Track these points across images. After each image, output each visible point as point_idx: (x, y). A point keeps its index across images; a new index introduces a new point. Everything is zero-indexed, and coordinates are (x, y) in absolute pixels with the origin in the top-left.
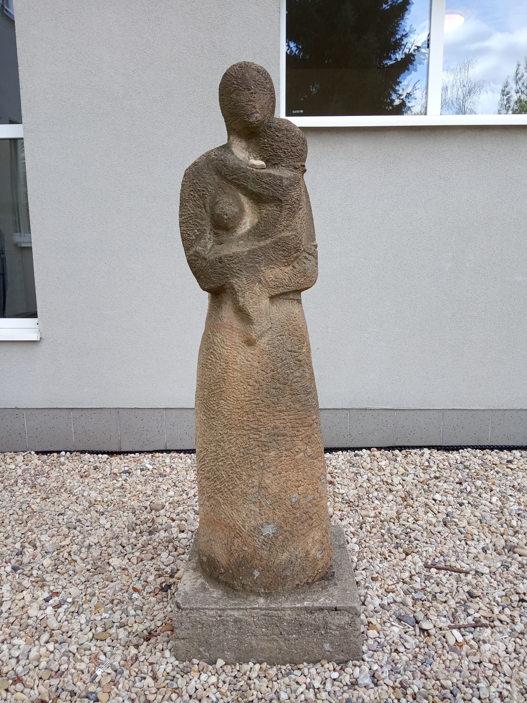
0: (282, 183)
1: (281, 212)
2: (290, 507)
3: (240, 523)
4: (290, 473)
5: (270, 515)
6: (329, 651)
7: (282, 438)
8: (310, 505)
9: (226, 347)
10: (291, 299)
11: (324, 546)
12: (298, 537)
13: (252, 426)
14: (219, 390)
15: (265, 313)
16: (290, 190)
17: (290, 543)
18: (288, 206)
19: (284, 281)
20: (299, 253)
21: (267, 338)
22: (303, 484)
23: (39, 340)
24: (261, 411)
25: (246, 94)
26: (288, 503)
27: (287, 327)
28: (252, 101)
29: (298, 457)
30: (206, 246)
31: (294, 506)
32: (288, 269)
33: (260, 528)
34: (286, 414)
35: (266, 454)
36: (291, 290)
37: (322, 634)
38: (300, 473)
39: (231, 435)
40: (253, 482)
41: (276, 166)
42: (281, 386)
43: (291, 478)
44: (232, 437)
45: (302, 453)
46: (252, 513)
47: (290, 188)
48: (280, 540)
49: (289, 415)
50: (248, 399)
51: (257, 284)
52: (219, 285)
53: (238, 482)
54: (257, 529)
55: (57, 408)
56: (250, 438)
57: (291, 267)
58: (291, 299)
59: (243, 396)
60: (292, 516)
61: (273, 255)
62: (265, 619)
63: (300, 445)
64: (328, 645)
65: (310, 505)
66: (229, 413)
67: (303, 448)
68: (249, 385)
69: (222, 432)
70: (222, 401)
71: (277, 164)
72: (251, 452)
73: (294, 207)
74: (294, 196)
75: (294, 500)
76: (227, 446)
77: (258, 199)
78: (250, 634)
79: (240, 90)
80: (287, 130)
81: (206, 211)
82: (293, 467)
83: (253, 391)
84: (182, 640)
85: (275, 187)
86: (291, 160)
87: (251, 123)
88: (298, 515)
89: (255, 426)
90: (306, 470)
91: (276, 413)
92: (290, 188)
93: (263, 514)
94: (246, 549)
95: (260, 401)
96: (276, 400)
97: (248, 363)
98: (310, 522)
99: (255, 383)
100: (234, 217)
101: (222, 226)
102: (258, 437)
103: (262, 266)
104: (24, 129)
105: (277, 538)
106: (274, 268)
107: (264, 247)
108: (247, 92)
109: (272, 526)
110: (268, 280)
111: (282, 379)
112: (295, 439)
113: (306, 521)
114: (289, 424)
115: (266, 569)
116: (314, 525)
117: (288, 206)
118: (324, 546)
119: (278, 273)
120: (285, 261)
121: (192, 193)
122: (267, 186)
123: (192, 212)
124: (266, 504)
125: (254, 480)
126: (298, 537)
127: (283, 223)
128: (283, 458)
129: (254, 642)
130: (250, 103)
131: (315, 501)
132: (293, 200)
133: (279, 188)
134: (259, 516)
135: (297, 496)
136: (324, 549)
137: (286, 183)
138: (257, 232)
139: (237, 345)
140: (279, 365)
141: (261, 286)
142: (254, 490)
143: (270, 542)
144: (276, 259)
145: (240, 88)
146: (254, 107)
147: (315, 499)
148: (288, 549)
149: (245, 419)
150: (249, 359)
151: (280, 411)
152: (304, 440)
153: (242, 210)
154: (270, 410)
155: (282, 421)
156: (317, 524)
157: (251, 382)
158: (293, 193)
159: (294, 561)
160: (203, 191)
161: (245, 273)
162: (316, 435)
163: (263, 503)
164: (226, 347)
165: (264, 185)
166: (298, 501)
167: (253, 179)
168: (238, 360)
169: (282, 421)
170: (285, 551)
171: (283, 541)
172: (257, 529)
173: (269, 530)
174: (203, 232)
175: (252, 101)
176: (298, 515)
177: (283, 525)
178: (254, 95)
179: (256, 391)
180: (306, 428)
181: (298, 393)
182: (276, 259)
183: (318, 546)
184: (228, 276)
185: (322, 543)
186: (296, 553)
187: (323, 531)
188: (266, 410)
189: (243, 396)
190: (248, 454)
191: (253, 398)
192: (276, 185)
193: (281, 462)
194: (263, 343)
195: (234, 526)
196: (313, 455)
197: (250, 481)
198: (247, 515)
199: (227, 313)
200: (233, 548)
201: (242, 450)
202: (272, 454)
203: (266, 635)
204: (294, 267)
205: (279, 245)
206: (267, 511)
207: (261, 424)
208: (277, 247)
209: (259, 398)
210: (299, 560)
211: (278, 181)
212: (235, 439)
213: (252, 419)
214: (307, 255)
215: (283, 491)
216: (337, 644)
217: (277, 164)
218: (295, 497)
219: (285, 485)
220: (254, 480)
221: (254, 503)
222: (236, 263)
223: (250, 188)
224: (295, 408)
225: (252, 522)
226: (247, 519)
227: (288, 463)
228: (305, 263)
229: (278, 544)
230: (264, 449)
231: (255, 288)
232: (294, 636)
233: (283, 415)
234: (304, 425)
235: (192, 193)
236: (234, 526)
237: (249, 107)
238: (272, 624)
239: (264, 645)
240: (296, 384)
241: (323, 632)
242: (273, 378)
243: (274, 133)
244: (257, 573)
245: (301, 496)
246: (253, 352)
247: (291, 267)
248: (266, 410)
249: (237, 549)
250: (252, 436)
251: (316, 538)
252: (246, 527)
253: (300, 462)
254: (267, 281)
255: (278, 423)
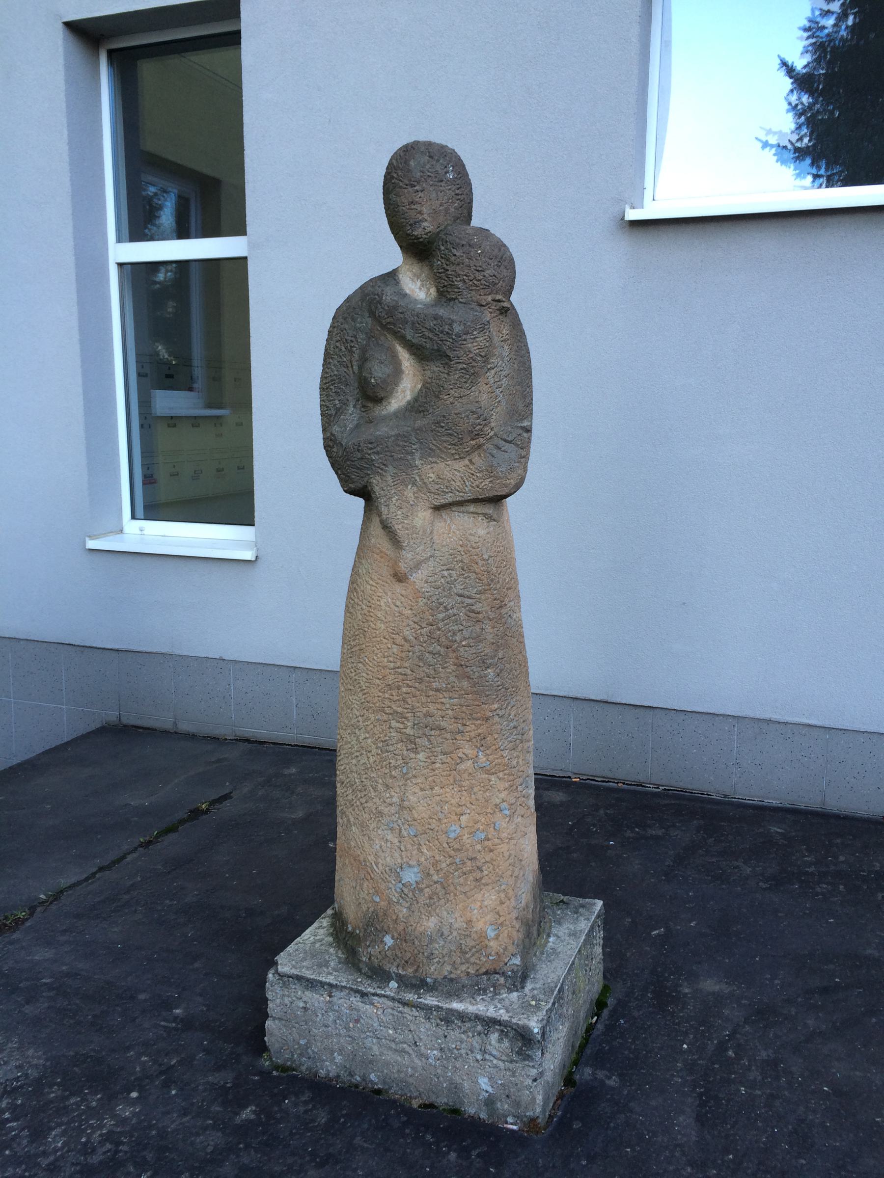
0: (451, 329)
1: (448, 374)
2: (445, 845)
3: (371, 858)
4: (448, 790)
5: (414, 853)
6: (487, 1092)
7: (438, 732)
8: (479, 847)
9: (371, 582)
10: (472, 513)
11: (502, 919)
12: (455, 895)
13: (395, 708)
14: (358, 648)
15: (421, 533)
16: (465, 340)
17: (442, 902)
18: (461, 366)
19: (453, 483)
20: (482, 440)
21: (425, 572)
22: (468, 811)
23: (254, 559)
24: (408, 686)
25: (408, 192)
26: (443, 838)
27: (459, 558)
28: (417, 203)
29: (462, 767)
30: (346, 427)
31: (451, 845)
32: (460, 465)
33: (398, 870)
34: (446, 696)
35: (412, 755)
36: (466, 498)
37: (477, 1060)
38: (464, 793)
39: (368, 719)
40: (391, 797)
41: (452, 303)
42: (442, 650)
43: (449, 798)
44: (369, 722)
45: (470, 762)
46: (389, 844)
47: (464, 337)
48: (427, 895)
49: (450, 698)
50: (392, 665)
51: (409, 487)
52: (360, 486)
53: (373, 794)
54: (396, 872)
55: (111, 650)
56: (390, 727)
57: (466, 462)
58: (472, 513)
59: (386, 660)
60: (449, 861)
61: (434, 442)
62: (393, 1015)
63: (468, 750)
64: (486, 1080)
65: (479, 847)
66: (367, 684)
67: (471, 752)
68: (394, 643)
69: (358, 714)
70: (360, 665)
71: (454, 299)
72: (391, 748)
73: (473, 367)
74: (472, 350)
75: (452, 835)
76: (363, 736)
77: (419, 353)
78: (371, 1034)
79: (401, 187)
80: (470, 245)
81: (354, 373)
82: (452, 781)
83: (400, 654)
84: (277, 1022)
85: (441, 335)
86: (474, 293)
87: (417, 238)
88: (457, 860)
89: (399, 710)
90: (475, 789)
91: (431, 693)
92: (464, 337)
93: (403, 848)
94: (378, 899)
95: (409, 672)
96: (432, 672)
97: (396, 609)
98: (478, 875)
99: (403, 642)
100: (384, 381)
101: (372, 396)
102: (402, 726)
103: (417, 458)
104: (249, 243)
105: (421, 890)
106: (435, 462)
107: (420, 429)
108: (410, 189)
109: (416, 870)
110: (425, 481)
111: (443, 639)
112: (459, 737)
113: (470, 872)
114: (450, 712)
115: (403, 938)
116: (483, 881)
117: (461, 366)
118: (502, 919)
119: (454, 473)
120: (454, 452)
121: (338, 344)
122: (431, 335)
123: (336, 373)
124: (409, 834)
125: (393, 793)
126: (455, 895)
127: (452, 392)
128: (438, 765)
129: (375, 1048)
130: (413, 207)
131: (489, 843)
132: (471, 356)
133: (445, 337)
134: (398, 850)
135: (458, 830)
136: (502, 924)
137: (457, 328)
138: (417, 407)
139: (385, 579)
140: (441, 616)
141: (415, 489)
142: (393, 809)
143: (410, 895)
144: (440, 449)
145: (401, 184)
146: (420, 213)
147: (489, 840)
148: (437, 911)
149: (387, 696)
150: (398, 603)
151: (437, 690)
152: (474, 740)
153: (398, 372)
154: (423, 686)
155: (439, 706)
156: (490, 881)
157: (399, 640)
158: (470, 345)
159: (446, 933)
160: (352, 341)
161: (390, 467)
162: (496, 736)
163: (403, 831)
164: (371, 582)
165: (426, 334)
166: (458, 838)
167: (413, 323)
168: (382, 604)
169: (439, 706)
170: (433, 913)
171: (431, 898)
172: (396, 872)
173: (410, 876)
174: (345, 403)
175: (417, 203)
176: (457, 860)
177: (432, 872)
178: (420, 194)
179: (404, 655)
180: (479, 722)
181: (467, 664)
182: (440, 449)
183: (490, 917)
184: (369, 472)
185: (498, 913)
186: (451, 921)
187: (502, 895)
188: (417, 685)
189: (386, 660)
190: (387, 752)
191: (398, 664)
192: (442, 332)
193: (434, 770)
194: (418, 578)
195: (365, 861)
196: (488, 768)
197: (388, 795)
198: (381, 847)
199: (376, 528)
200: (362, 895)
201: (380, 745)
202: (421, 756)
203: (394, 1041)
204: (470, 461)
205: (442, 427)
206: (409, 846)
207: (407, 706)
208: (440, 429)
209: (406, 665)
210: (455, 933)
211: (447, 327)
212: (372, 726)
213: (396, 698)
214: (502, 443)
215: (435, 817)
216: (500, 1082)
217: (454, 299)
218: (454, 830)
219: (439, 808)
220: (393, 793)
221: (392, 829)
222: (378, 453)
223: (409, 337)
224: (462, 688)
225: (388, 859)
226: (381, 853)
227: (444, 774)
228: (493, 456)
229: (423, 900)
230: (409, 747)
231: (405, 493)
232: (435, 1052)
233: (441, 696)
234: (475, 716)
235: (338, 344)
236: (365, 861)
237: (412, 213)
238: (403, 1025)
239: (390, 1056)
240: (467, 649)
241: (479, 1057)
242: (430, 635)
243: (450, 251)
244: (389, 940)
245: (466, 831)
246: (404, 592)
247: (466, 462)
248: (417, 685)
249: (367, 897)
250: (394, 724)
251: (486, 903)
252: (380, 866)
253: (466, 776)
254: (425, 483)
255: (432, 708)
